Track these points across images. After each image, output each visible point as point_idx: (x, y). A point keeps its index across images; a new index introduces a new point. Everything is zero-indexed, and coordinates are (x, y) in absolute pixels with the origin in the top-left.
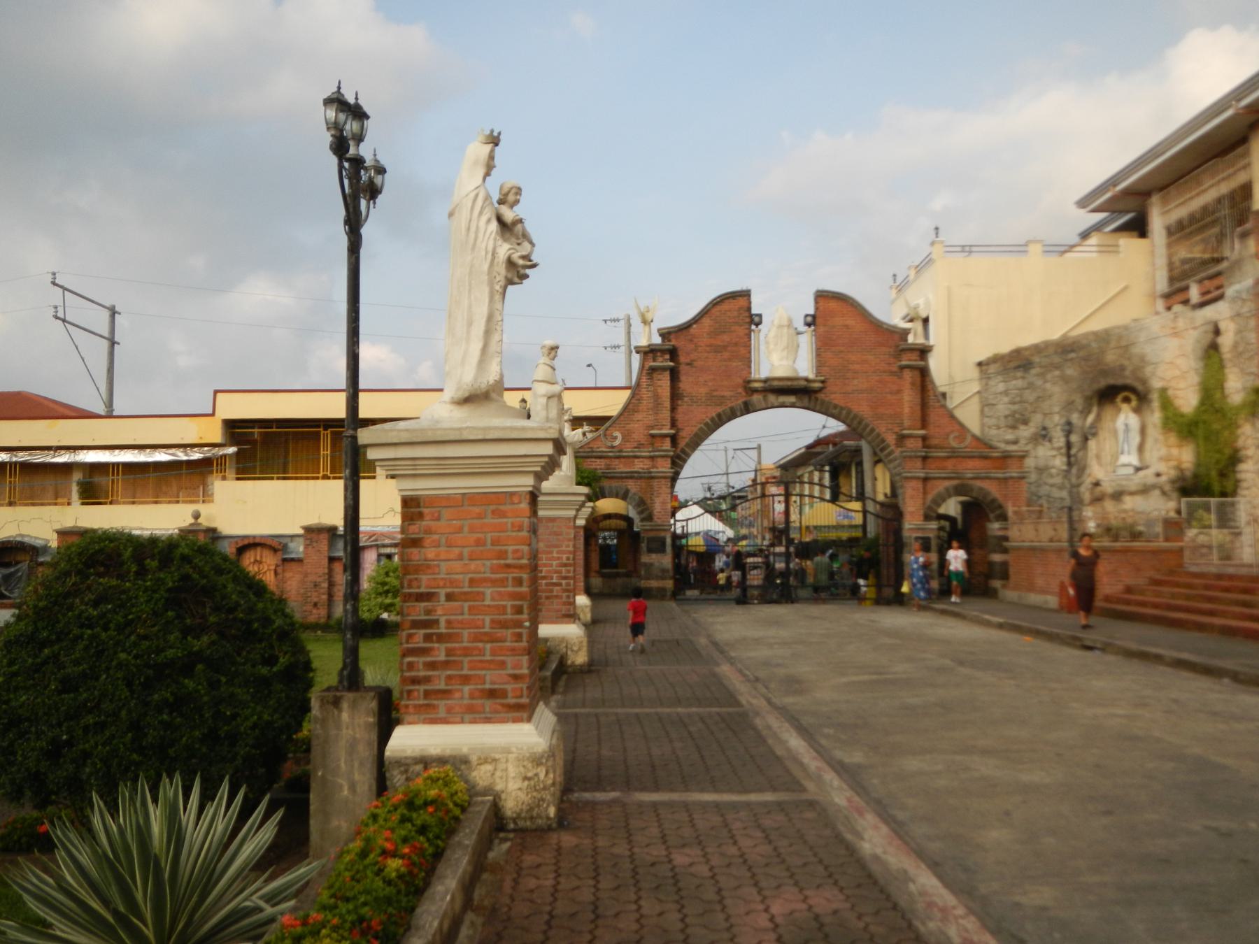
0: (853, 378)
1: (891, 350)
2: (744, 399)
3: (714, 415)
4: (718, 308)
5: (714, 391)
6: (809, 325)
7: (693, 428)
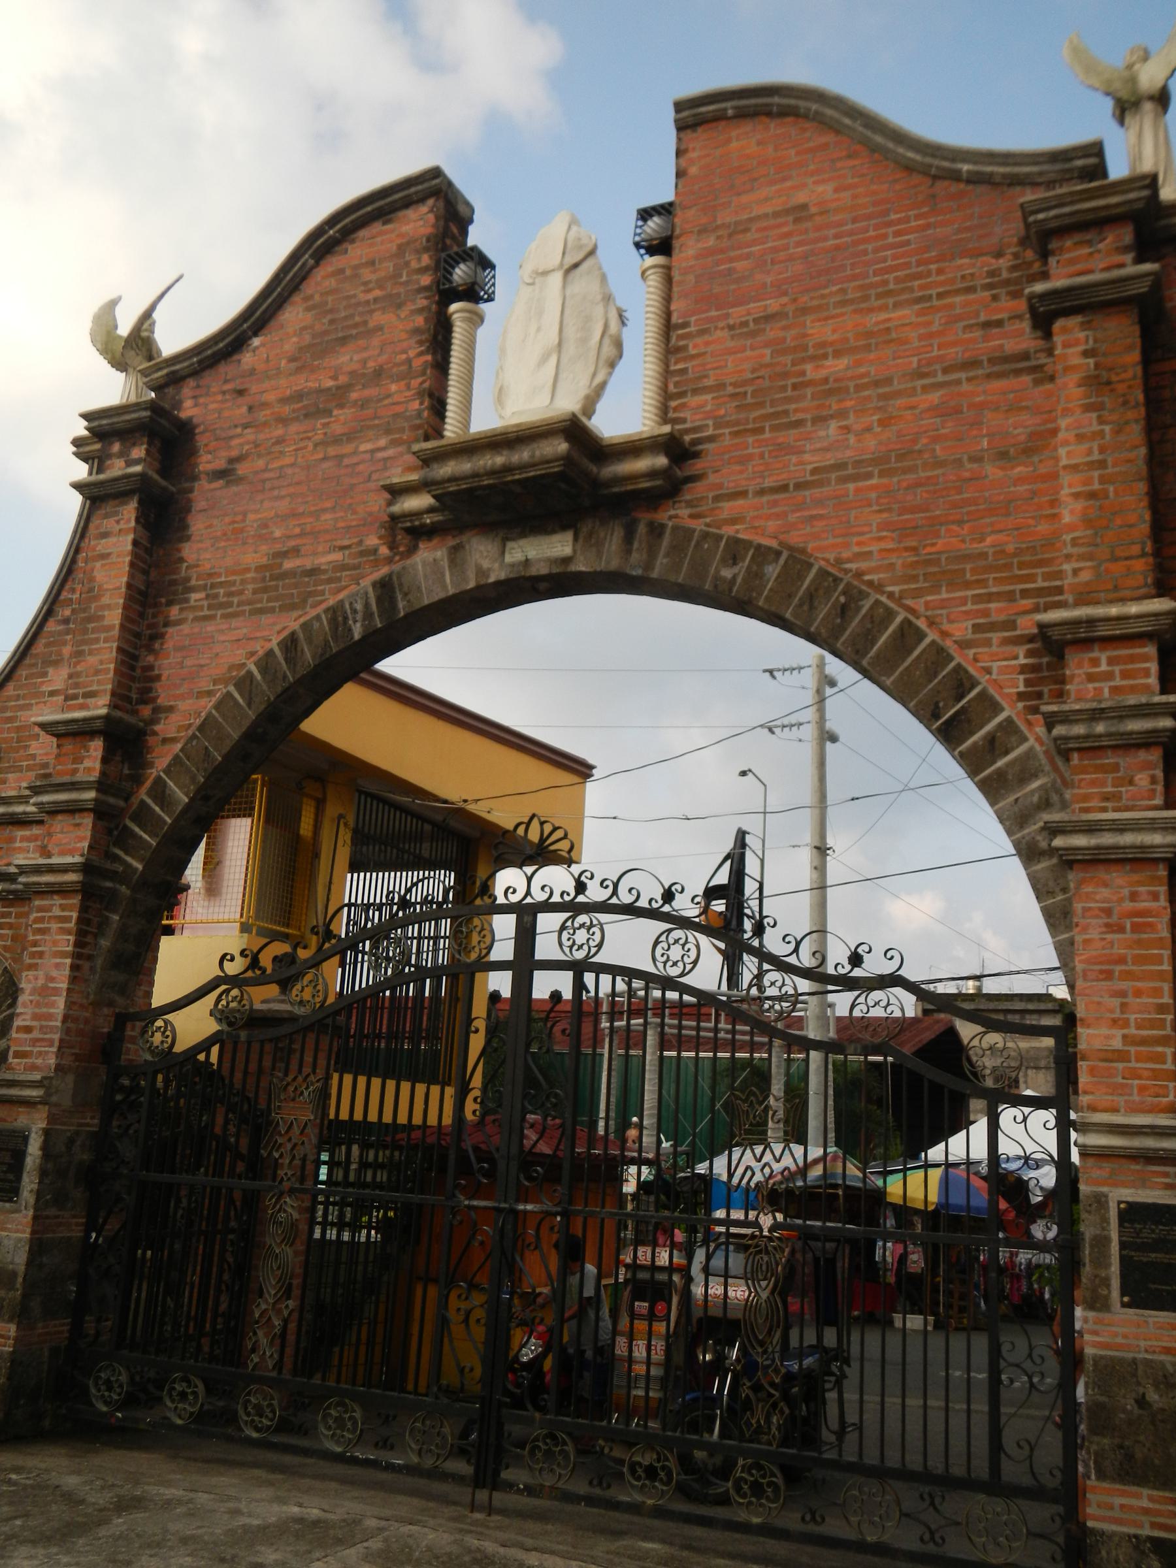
0: (820, 420)
1: (1004, 263)
2: (384, 571)
3: (274, 644)
4: (334, 262)
5: (284, 554)
6: (660, 246)
7: (203, 701)
